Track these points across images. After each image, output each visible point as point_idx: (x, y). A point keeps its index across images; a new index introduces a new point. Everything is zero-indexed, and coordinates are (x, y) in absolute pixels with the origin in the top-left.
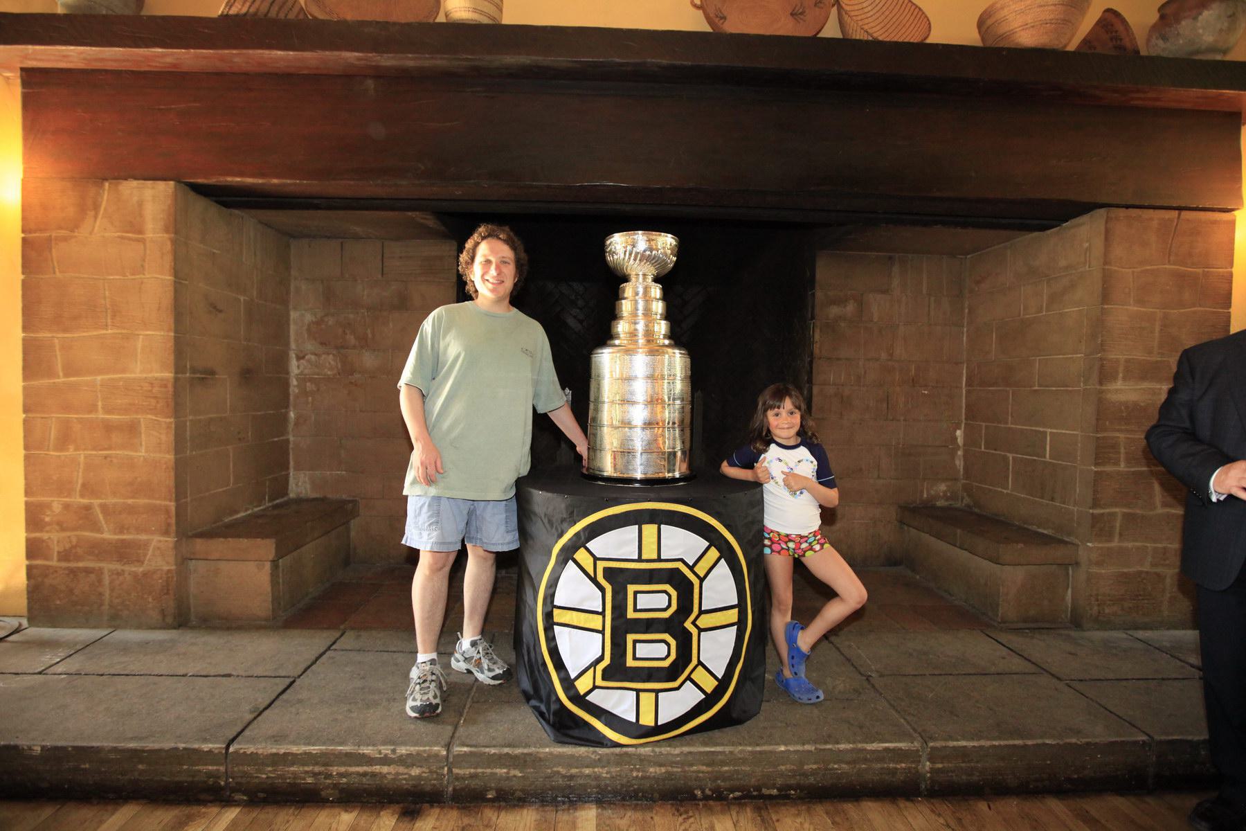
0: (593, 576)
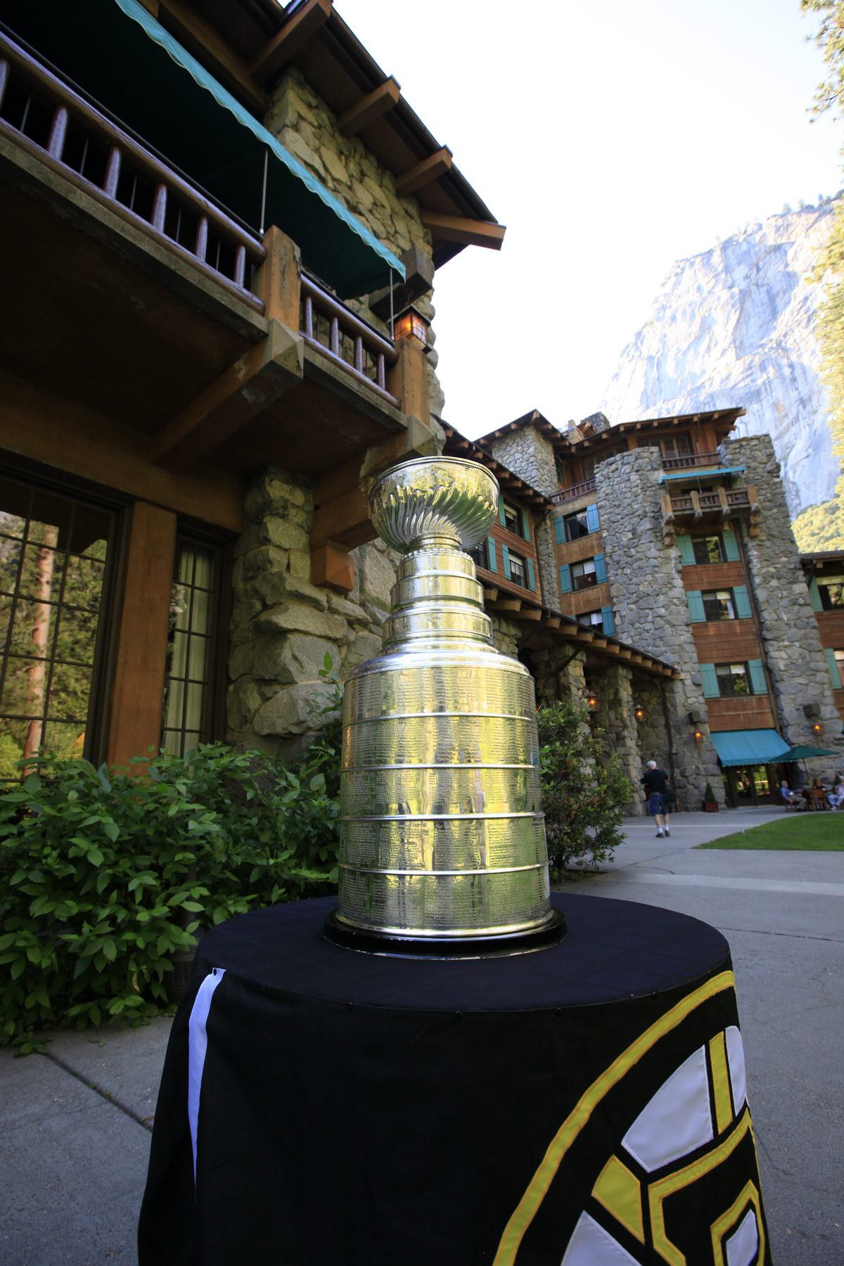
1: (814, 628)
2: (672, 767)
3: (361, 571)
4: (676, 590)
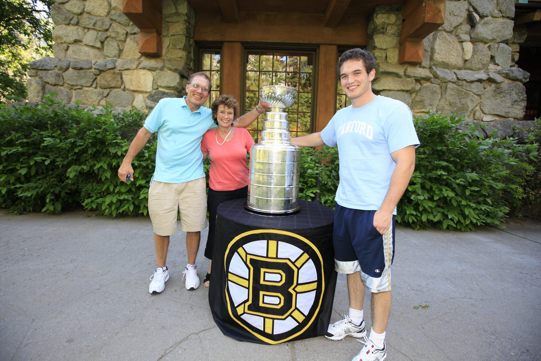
0: (245, 260)
3: (432, 49)
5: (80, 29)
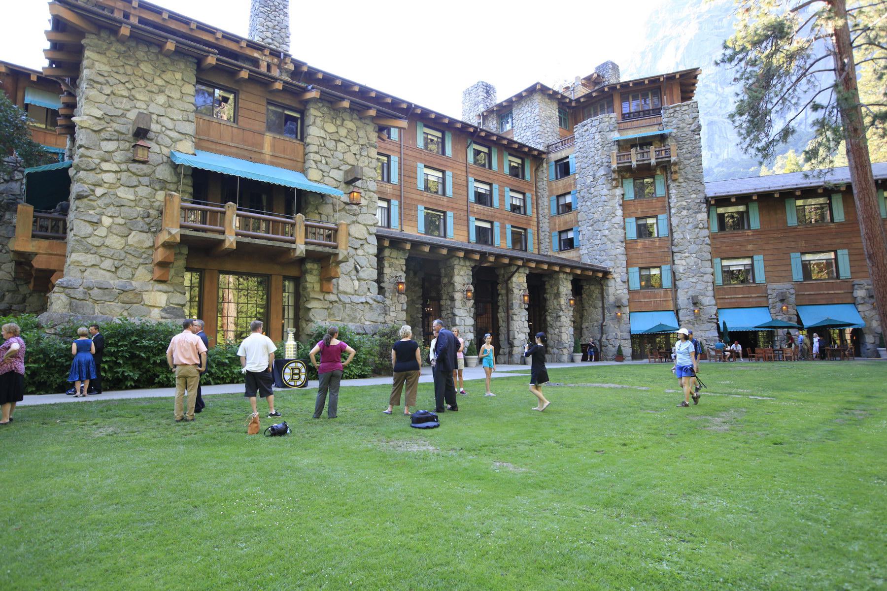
1: (707, 244)
2: (602, 334)
3: (338, 283)
4: (617, 218)
5: (98, 257)
